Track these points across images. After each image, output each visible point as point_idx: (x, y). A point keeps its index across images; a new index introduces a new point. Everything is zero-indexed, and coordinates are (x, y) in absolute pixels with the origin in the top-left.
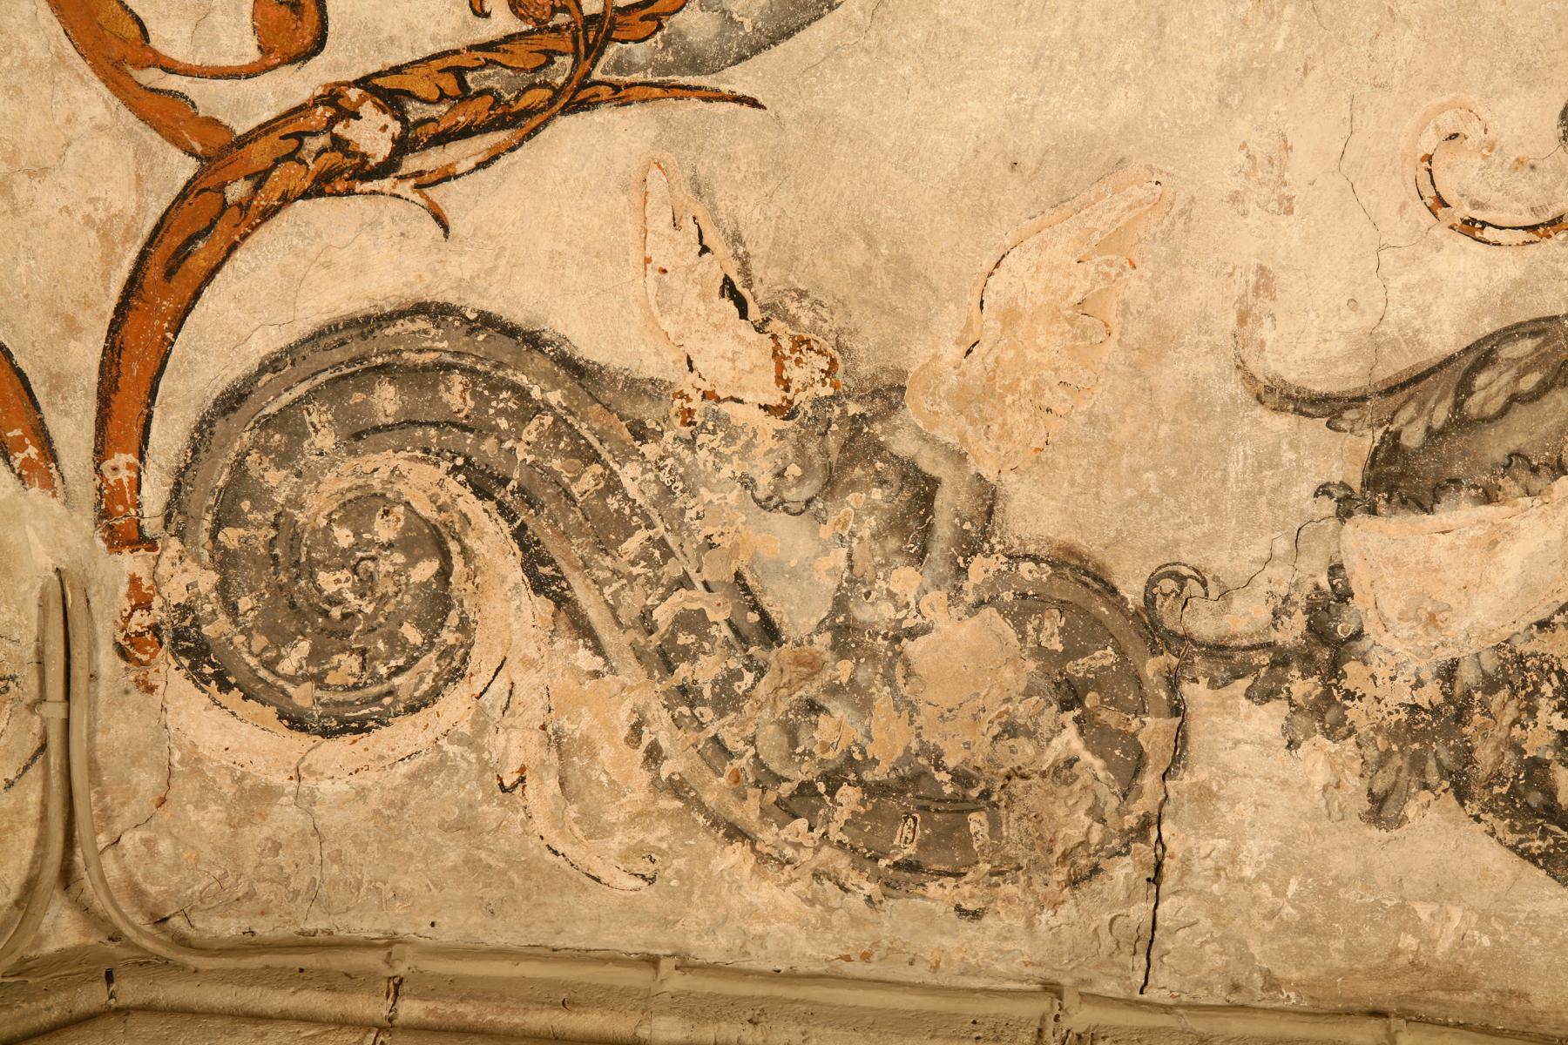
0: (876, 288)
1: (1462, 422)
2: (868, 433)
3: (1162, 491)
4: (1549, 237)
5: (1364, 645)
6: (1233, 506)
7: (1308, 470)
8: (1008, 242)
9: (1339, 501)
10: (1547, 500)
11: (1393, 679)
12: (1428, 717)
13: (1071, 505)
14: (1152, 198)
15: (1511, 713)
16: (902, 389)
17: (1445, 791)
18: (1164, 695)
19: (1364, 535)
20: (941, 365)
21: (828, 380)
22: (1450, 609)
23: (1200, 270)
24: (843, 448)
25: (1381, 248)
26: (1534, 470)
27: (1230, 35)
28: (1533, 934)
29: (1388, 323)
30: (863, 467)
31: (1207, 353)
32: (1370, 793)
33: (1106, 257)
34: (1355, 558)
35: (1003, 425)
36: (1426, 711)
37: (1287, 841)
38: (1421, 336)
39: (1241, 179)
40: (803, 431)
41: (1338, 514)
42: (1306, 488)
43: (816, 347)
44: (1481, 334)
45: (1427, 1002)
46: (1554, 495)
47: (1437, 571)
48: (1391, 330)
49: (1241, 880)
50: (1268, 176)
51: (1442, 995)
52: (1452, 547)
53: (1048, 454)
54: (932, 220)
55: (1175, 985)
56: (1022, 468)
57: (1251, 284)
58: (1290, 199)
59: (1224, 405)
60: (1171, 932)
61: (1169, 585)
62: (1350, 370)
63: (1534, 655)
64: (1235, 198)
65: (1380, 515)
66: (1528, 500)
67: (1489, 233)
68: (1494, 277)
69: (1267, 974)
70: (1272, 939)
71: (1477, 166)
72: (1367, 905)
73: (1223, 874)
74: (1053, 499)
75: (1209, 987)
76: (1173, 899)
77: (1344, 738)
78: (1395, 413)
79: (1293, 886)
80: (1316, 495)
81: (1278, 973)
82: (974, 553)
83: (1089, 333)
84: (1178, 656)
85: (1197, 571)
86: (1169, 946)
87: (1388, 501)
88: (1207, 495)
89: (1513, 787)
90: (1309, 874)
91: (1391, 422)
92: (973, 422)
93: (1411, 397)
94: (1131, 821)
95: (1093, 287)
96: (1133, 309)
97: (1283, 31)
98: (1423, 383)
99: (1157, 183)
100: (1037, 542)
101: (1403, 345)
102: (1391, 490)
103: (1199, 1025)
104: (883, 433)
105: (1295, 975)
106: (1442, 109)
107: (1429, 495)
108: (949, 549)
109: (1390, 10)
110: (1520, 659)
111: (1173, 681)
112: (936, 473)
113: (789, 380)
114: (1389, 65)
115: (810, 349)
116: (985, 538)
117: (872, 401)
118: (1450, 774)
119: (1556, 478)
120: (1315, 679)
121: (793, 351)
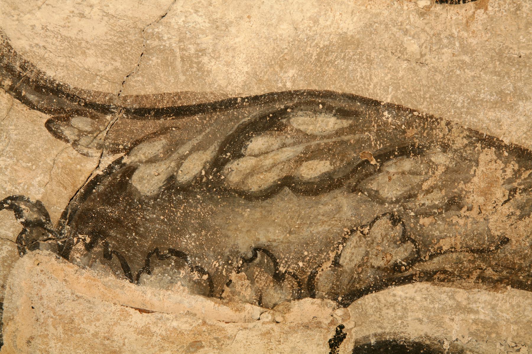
9: (26, 224)
10: (279, 319)
19: (42, 277)
26: (278, 278)
29: (168, 25)
34: (20, 302)
38: (205, 59)
41: (19, 240)
44: (278, 87)
46: (290, 317)
52: (145, 332)
62: (101, 66)
65: (72, 261)
66: (257, 310)
68: (321, 21)
87: (89, 247)
91: (128, 151)
93: (164, 131)
101: (178, 63)
107: (141, 260)
119: (299, 298)
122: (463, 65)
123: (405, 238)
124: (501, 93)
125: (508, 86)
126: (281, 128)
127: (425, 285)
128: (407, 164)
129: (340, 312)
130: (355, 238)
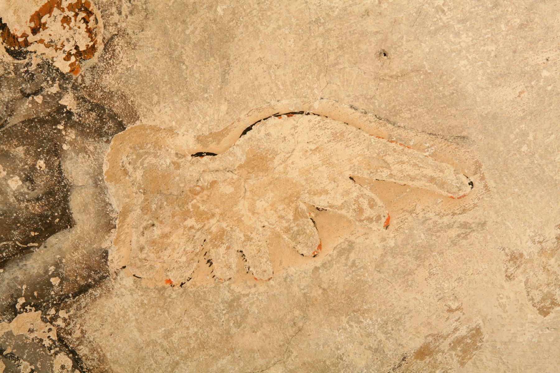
0: (183, 31)
2: (60, 131)
8: (316, 106)
13: (148, 350)
14: (456, 190)
16: (121, 127)
20: (169, 141)
21: (73, 59)
23: (432, 282)
24: (28, 122)
30: (27, 152)
31: (370, 348)
33: (373, 196)
35: (165, 236)
39: (535, 249)
40: (12, 75)
43: (91, 24)
53: (174, 293)
54: (279, 28)
56: (143, 283)
57: (457, 334)
74: (141, 331)
82: (37, 307)
83: (300, 239)
92: (145, 209)
95: (341, 208)
96: (352, 256)
99: (471, 184)
100: (93, 350)
104: (71, 143)
108: (22, 283)
112: (76, 216)
113: (44, 26)
115: (86, 21)
116: (58, 305)
117: (88, 111)
121: (71, 7)
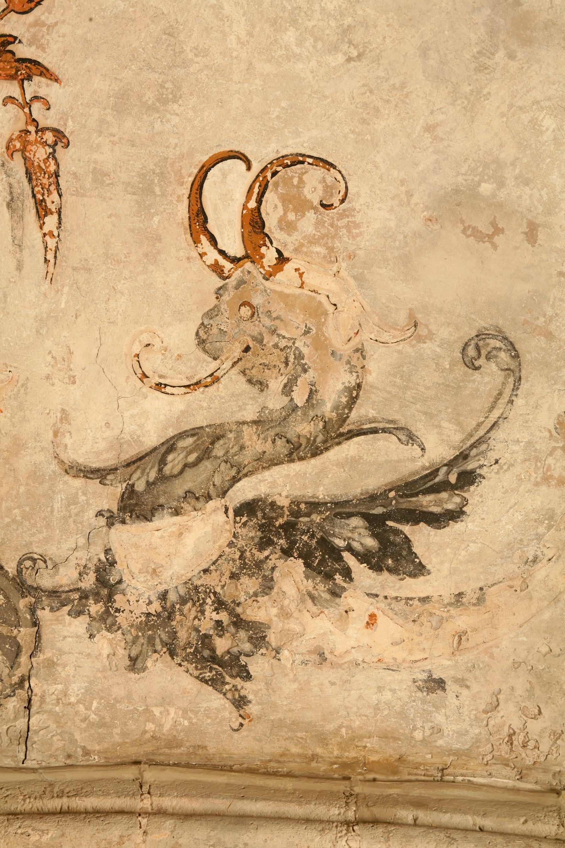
1: (162, 478)
3: (23, 518)
4: (196, 390)
5: (123, 586)
6: (57, 524)
7: (91, 505)
9: (107, 518)
11: (137, 601)
12: (155, 618)
15: (193, 613)
17: (165, 653)
18: (29, 617)
22: (162, 566)
23: (33, 412)
25: (119, 398)
26: (197, 499)
27: (38, 301)
28: (208, 717)
29: (125, 433)
32: (130, 656)
36: (154, 616)
37: (91, 683)
38: (141, 438)
41: (107, 525)
42: (91, 513)
45: (160, 755)
46: (207, 510)
47: (155, 549)
48: (127, 437)
49: (70, 704)
50: (63, 367)
51: (167, 751)
52: (162, 537)
55: (40, 758)
58: (74, 377)
59: (50, 475)
60: (36, 732)
61: (28, 563)
63: (202, 585)
64: (48, 377)
66: (195, 513)
67: (168, 389)
69: (84, 748)
70: (85, 731)
71: (160, 359)
72: (130, 711)
73: (60, 701)
75: (56, 757)
76: (37, 716)
77: (116, 631)
78: (131, 475)
79: (95, 704)
80: (96, 516)
81: (89, 748)
84: (34, 597)
85: (41, 556)
86: (36, 739)
87: (131, 517)
88: (44, 519)
89: (196, 648)
90: (102, 698)
91: (130, 479)
93: (138, 467)
94: (15, 679)
97: (64, 298)
98: (143, 461)
101: (133, 443)
102: (131, 512)
103: (50, 777)
105: (97, 748)
106: (142, 332)
107: (149, 513)
109: (113, 287)
110: (196, 588)
111: (33, 610)
114: (115, 313)
118: (167, 644)
119: (207, 502)
120: (101, 604)
122: (223, 403)
123: (232, 466)
124: (239, 406)
125: (240, 403)
126: (175, 449)
127: (246, 479)
128: (221, 442)
129: (223, 500)
130: (216, 474)
